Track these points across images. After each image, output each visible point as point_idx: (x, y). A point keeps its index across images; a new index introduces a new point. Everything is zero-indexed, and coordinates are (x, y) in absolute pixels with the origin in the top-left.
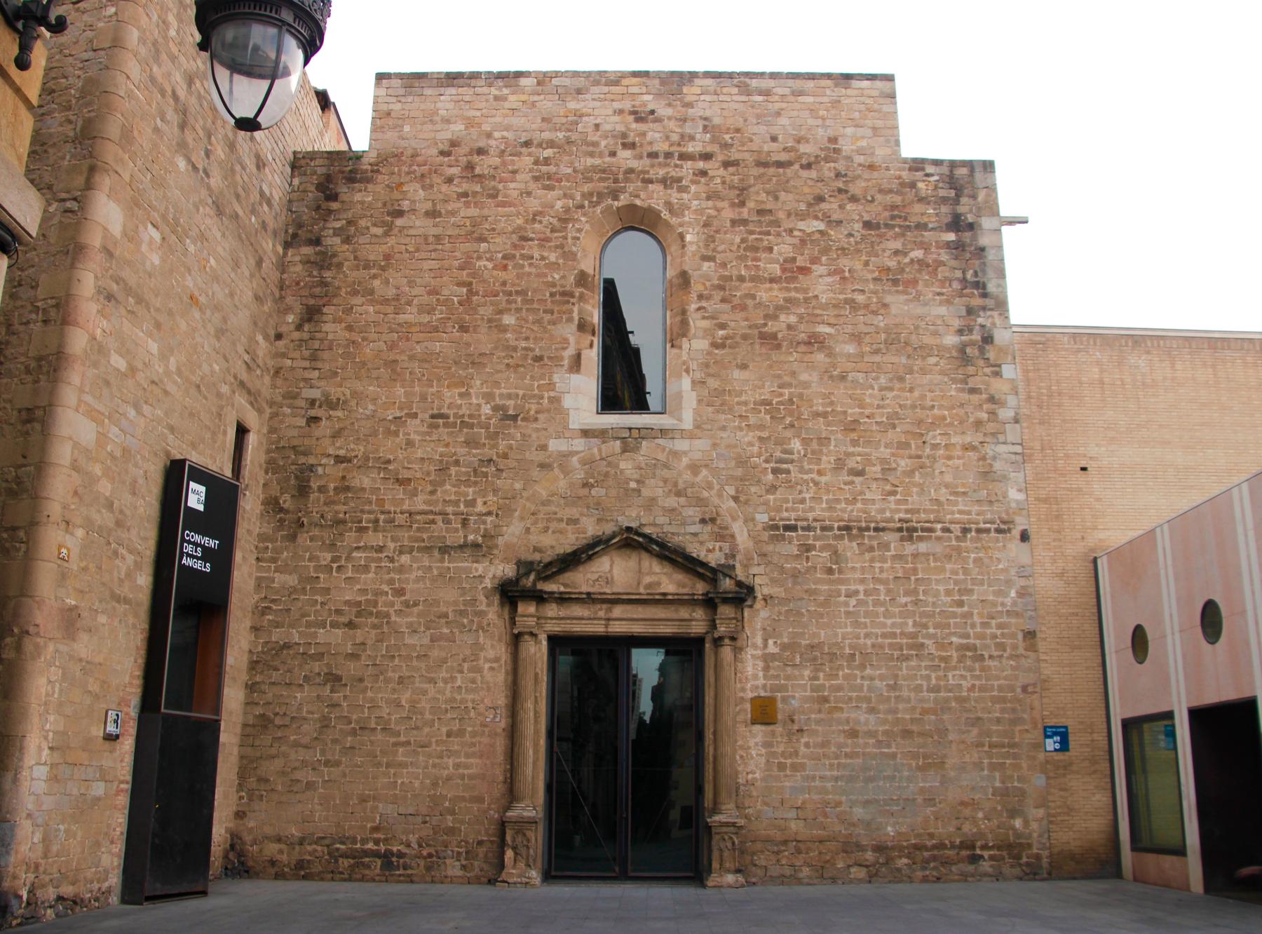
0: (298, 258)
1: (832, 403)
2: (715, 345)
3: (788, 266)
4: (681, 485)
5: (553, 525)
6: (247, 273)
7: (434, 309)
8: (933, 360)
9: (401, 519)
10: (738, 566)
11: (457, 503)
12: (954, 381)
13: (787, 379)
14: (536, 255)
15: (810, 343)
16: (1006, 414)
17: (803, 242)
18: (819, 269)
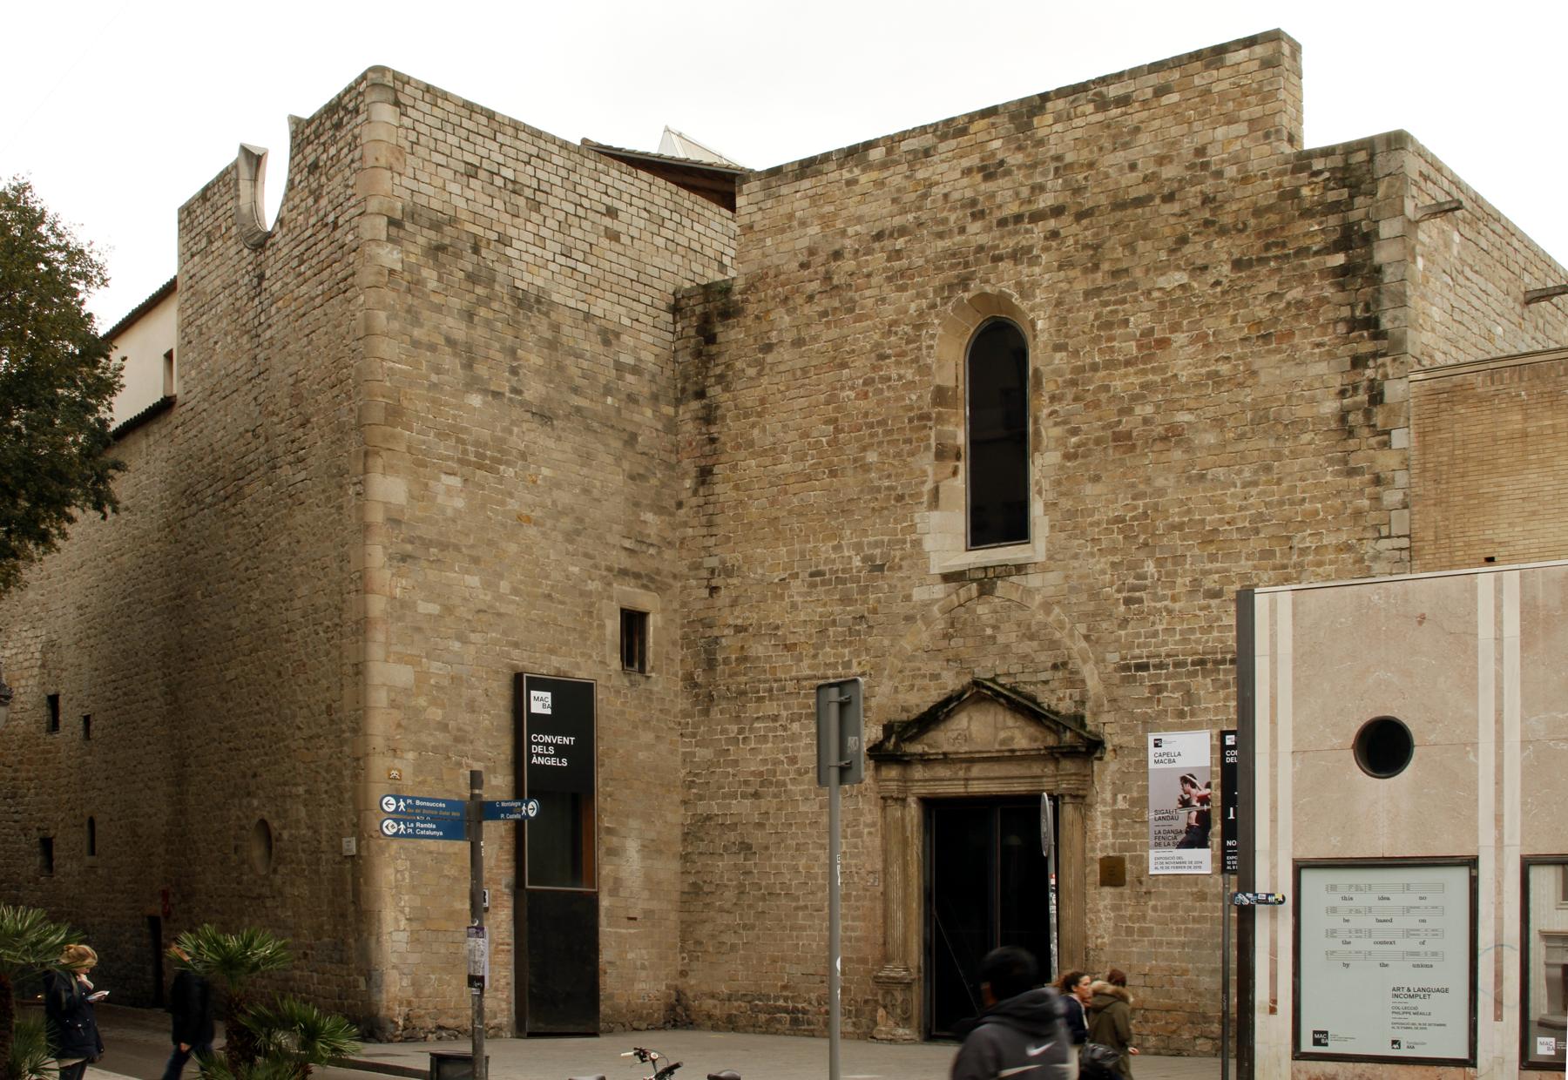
0: (688, 415)
1: (1189, 511)
2: (1068, 457)
3: (1145, 341)
4: (1033, 629)
5: (918, 682)
6: (610, 459)
7: (806, 455)
8: (1306, 438)
9: (790, 686)
10: (1088, 715)
11: (834, 666)
12: (1330, 461)
13: (1142, 487)
14: (894, 376)
15: (1165, 439)
16: (1392, 497)
17: (1162, 304)
18: (1180, 338)
